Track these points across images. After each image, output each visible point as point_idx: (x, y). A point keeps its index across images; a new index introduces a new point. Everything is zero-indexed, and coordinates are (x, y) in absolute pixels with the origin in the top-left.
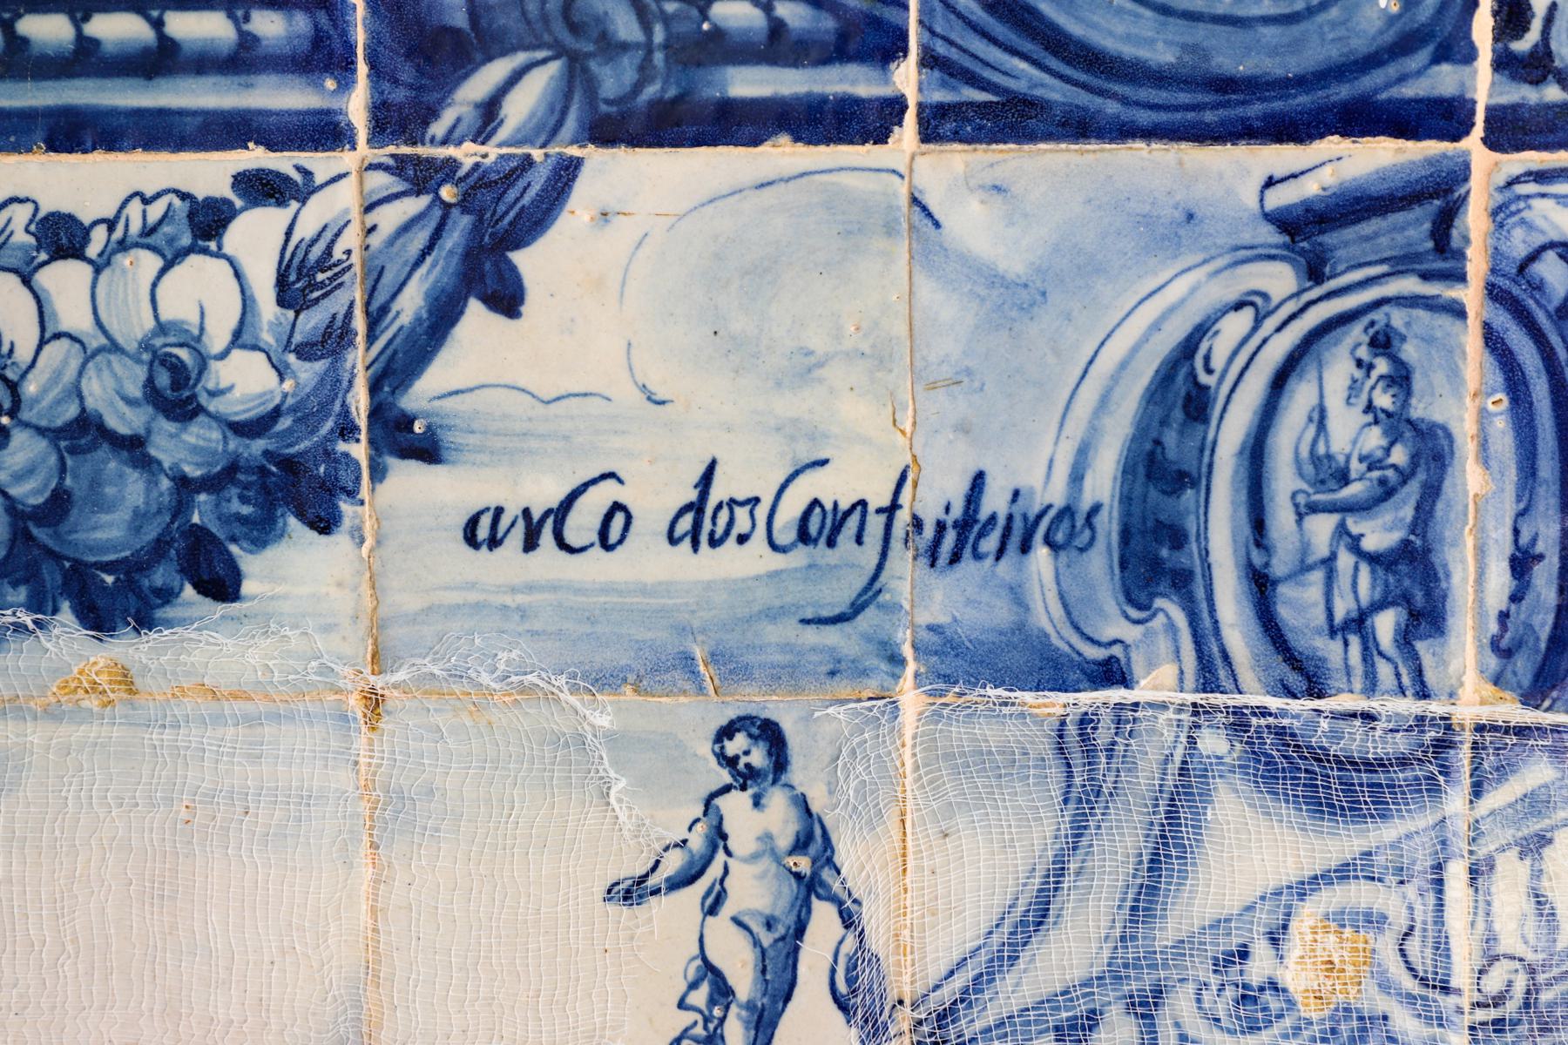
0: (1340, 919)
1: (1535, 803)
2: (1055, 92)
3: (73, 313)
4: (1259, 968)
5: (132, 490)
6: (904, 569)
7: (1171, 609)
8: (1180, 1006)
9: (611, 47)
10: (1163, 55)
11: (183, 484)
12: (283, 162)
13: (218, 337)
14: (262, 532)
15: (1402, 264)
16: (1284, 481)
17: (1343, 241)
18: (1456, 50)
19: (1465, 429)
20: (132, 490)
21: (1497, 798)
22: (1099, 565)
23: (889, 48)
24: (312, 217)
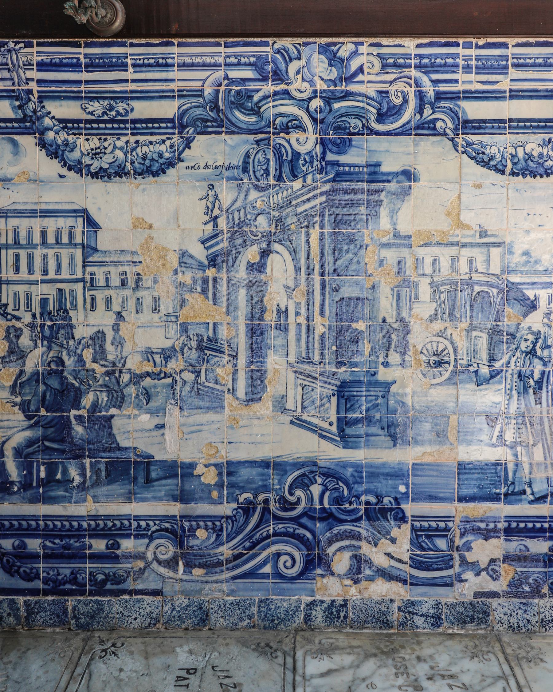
0: (261, 201)
1: (278, 190)
2: (236, 130)
3: (152, 149)
4: (254, 205)
5: (157, 165)
6: (224, 170)
7: (247, 174)
8: (248, 208)
9: (198, 126)
10: (245, 127)
11: (161, 164)
12: (170, 136)
13: (164, 151)
14: (168, 168)
15: (265, 145)
16: (256, 163)
17: (261, 143)
18: (269, 127)
19: (271, 159)
20: (157, 165)
21: (274, 190)
22: (241, 170)
23: (223, 126)
24: (173, 141)
